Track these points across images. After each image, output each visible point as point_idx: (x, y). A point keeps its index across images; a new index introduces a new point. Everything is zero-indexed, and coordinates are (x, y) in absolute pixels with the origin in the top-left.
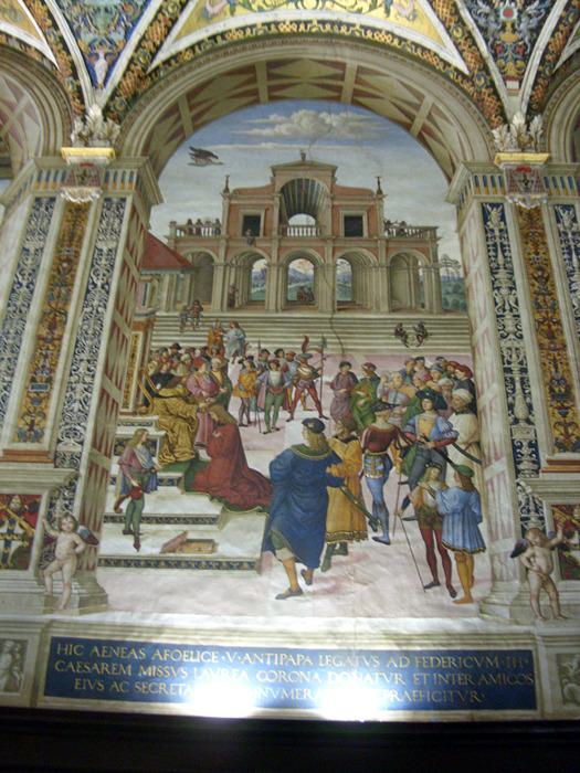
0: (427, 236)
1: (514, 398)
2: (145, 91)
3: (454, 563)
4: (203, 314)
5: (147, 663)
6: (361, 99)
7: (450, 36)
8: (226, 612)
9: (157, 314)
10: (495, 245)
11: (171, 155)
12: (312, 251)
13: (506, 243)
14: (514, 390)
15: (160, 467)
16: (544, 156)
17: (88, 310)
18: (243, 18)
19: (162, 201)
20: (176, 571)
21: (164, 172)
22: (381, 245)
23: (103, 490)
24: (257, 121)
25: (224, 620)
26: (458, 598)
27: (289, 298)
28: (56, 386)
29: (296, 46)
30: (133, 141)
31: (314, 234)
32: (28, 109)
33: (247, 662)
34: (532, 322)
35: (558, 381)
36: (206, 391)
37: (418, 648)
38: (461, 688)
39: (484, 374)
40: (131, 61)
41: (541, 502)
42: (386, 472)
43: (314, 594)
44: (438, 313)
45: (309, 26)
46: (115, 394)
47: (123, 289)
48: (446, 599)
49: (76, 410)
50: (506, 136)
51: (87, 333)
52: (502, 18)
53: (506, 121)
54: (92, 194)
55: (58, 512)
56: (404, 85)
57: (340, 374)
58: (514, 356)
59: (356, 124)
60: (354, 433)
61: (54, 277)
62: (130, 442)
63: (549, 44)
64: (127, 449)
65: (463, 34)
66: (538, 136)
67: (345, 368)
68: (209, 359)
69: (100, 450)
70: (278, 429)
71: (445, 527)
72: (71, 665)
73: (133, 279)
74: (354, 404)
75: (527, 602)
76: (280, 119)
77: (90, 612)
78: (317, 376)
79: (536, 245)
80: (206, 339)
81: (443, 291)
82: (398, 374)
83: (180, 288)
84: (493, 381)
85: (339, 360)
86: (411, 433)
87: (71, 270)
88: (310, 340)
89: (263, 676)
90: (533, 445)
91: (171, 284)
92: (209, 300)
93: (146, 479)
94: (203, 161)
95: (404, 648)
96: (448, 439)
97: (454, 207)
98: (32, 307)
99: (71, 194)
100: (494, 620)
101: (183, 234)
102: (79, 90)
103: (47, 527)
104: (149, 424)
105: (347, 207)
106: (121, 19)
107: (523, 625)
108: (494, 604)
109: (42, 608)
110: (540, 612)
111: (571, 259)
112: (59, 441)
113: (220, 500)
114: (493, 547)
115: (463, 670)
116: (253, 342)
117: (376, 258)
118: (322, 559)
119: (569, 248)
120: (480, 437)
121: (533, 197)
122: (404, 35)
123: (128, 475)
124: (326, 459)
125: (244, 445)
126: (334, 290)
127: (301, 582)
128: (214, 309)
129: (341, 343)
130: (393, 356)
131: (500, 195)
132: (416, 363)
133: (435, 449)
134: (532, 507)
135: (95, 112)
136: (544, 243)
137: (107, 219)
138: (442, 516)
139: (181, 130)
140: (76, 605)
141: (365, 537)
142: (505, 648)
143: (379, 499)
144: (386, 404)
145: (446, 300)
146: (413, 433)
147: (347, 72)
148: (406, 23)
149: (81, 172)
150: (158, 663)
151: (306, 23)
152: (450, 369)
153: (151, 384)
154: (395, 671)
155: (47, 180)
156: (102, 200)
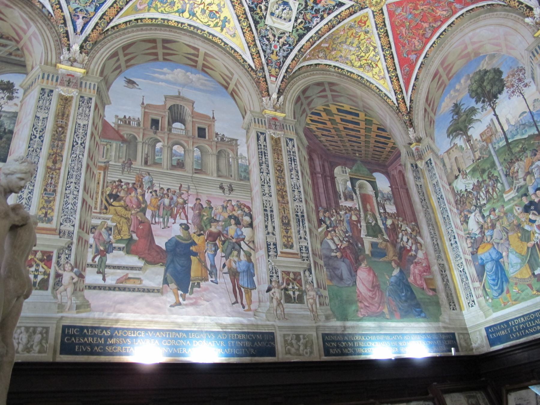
0: (233, 143)
4: (133, 166)
5: (111, 337)
6: (206, 69)
7: (250, 50)
9: (110, 163)
11: (115, 79)
14: (268, 219)
17: (74, 156)
18: (153, 14)
19: (110, 103)
20: (123, 293)
21: (111, 88)
30: (95, 67)
32: (34, 34)
37: (230, 330)
38: (247, 348)
40: (97, 24)
42: (216, 251)
43: (186, 305)
46: (89, 201)
48: (241, 309)
49: (70, 208)
52: (273, 48)
54: (73, 92)
55: (63, 261)
56: (225, 66)
58: (268, 204)
59: (204, 81)
60: (202, 232)
61: (54, 135)
62: (98, 227)
63: (290, 64)
67: (198, 201)
68: (136, 189)
72: (73, 339)
73: (97, 143)
74: (202, 218)
76: (169, 71)
77: (81, 312)
78: (186, 203)
79: (278, 155)
89: (165, 342)
90: (275, 244)
91: (116, 148)
92: (135, 159)
93: (107, 246)
94: (131, 86)
95: (225, 330)
96: (241, 238)
97: (245, 131)
98: (42, 150)
99: (63, 91)
102: (67, 32)
103: (57, 268)
105: (199, 123)
108: (259, 312)
109: (57, 310)
111: (291, 164)
112: (61, 224)
113: (143, 259)
115: (248, 340)
117: (212, 151)
118: (189, 289)
119: (291, 158)
122: (227, 42)
123: (98, 244)
125: (154, 233)
127: (181, 299)
128: (138, 164)
129: (196, 189)
131: (264, 129)
133: (236, 242)
134: (274, 271)
135: (76, 47)
136: (281, 155)
138: (239, 273)
139: (119, 67)
141: (207, 280)
142: (264, 331)
144: (216, 220)
146: (227, 234)
148: (230, 38)
149: (68, 79)
150: (116, 337)
151: (182, 24)
152: (242, 207)
153: (108, 199)
155: (48, 79)
156: (79, 97)
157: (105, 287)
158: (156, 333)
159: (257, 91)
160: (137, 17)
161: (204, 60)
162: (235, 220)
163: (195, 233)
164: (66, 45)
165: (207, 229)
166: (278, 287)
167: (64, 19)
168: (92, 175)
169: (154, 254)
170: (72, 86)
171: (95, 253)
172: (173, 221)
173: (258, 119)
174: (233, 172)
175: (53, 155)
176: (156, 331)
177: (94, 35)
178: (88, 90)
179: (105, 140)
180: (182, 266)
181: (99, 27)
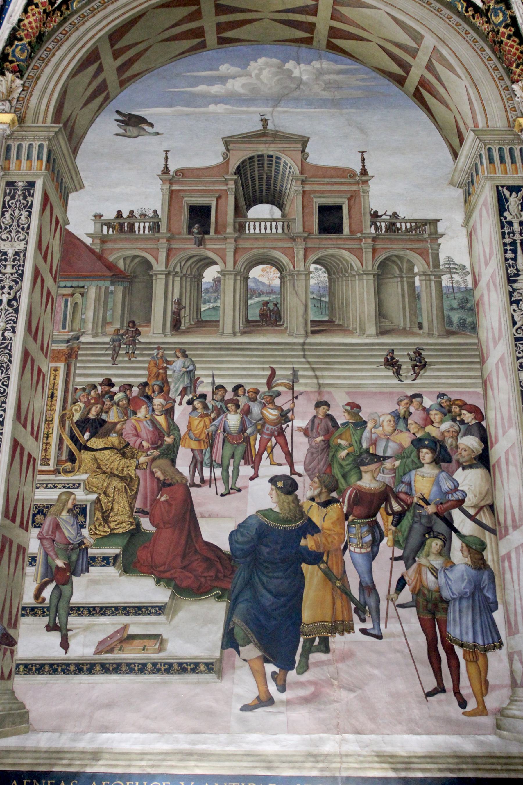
4: (141, 339)
9: (82, 339)
10: (513, 243)
11: (92, 121)
12: (277, 254)
15: (92, 541)
19: (82, 186)
20: (114, 677)
21: (83, 147)
22: (367, 244)
23: (19, 573)
26: (469, 708)
27: (250, 319)
30: (40, 100)
31: (280, 230)
36: (147, 441)
37: (420, 775)
39: (499, 416)
42: (375, 544)
43: (288, 703)
44: (440, 336)
47: (37, 310)
57: (315, 417)
60: (334, 494)
62: (52, 509)
67: (322, 410)
68: (149, 398)
69: (13, 520)
70: (239, 490)
71: (451, 616)
73: (49, 293)
74: (334, 456)
80: (146, 372)
81: (446, 307)
82: (389, 417)
83: (110, 305)
84: (510, 427)
86: (406, 493)
88: (278, 373)
91: (98, 299)
92: (148, 321)
93: (74, 557)
94: (133, 131)
95: (403, 774)
100: (515, 739)
101: (111, 232)
104: (76, 486)
108: (514, 717)
114: (512, 642)
116: (207, 376)
118: (297, 658)
120: (493, 498)
123: (51, 553)
124: (300, 528)
125: (197, 510)
126: (306, 306)
127: (272, 688)
129: (316, 377)
133: (436, 514)
137: (10, 211)
138: (448, 602)
139: (103, 87)
143: (367, 579)
144: (374, 455)
145: (449, 317)
146: (409, 494)
152: (456, 409)
157: (68, 665)
159: (496, 69)
162: (433, 451)
163: (312, 499)
165: (349, 486)
169: (199, 566)
173: (501, 150)
174: (425, 315)
177: (32, 19)
178: (24, 163)
179: (69, 284)
180: (277, 595)
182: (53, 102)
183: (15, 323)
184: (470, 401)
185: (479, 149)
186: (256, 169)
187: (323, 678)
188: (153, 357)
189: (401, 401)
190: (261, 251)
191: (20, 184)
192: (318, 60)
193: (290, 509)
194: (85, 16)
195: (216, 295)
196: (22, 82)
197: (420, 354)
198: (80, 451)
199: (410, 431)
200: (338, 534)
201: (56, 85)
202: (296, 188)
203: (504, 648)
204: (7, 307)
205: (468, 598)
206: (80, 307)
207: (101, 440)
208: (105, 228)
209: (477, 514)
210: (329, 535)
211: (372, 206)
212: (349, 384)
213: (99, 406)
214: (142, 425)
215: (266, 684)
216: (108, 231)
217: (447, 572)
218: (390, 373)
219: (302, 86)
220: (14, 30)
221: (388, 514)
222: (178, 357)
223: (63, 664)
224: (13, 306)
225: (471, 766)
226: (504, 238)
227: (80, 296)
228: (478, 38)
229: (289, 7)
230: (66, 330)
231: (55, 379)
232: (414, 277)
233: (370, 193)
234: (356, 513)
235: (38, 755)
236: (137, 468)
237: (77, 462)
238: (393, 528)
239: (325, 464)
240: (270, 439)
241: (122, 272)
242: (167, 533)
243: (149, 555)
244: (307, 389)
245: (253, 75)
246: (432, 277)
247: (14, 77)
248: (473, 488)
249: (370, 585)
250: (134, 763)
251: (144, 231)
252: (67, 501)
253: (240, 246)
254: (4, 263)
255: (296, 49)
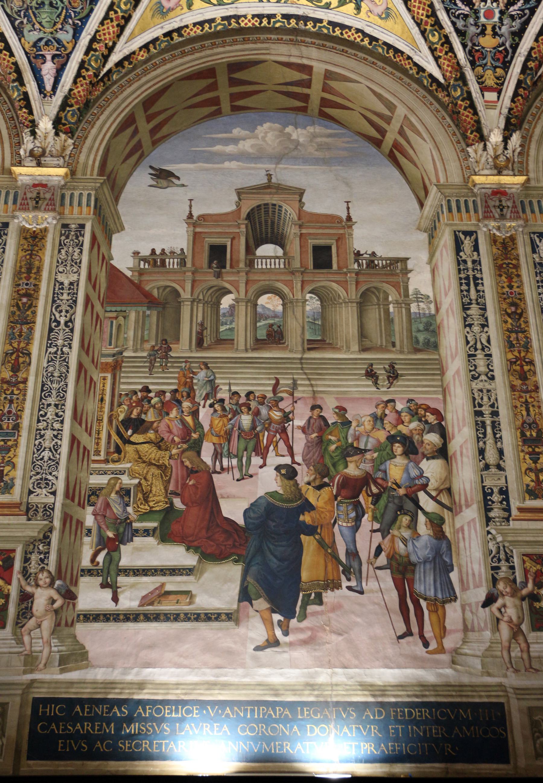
1: (485, 443)
2: (98, 98)
3: (426, 612)
4: (172, 354)
5: (130, 720)
8: (205, 664)
9: (125, 354)
10: (467, 278)
11: (130, 174)
12: (280, 285)
13: (478, 276)
14: (485, 434)
15: (135, 517)
16: (521, 179)
17: (53, 350)
19: (123, 229)
20: (154, 625)
23: (78, 542)
24: (220, 136)
25: (204, 674)
26: (431, 648)
28: (24, 433)
29: (259, 45)
30: (88, 156)
31: (282, 266)
33: (228, 716)
34: (504, 361)
35: (530, 425)
36: (178, 437)
37: (393, 700)
39: (455, 417)
40: (82, 65)
41: (512, 551)
42: (358, 519)
43: (291, 644)
44: (409, 353)
45: (272, 20)
46: (86, 440)
48: (419, 649)
49: (46, 459)
50: (481, 156)
51: (52, 376)
52: (483, 20)
53: (483, 139)
55: (33, 567)
57: (311, 417)
58: (485, 399)
60: (326, 480)
61: (13, 313)
62: (104, 491)
63: (532, 49)
64: (101, 499)
65: (440, 39)
66: (516, 154)
67: (316, 412)
68: (179, 402)
70: (251, 476)
71: (417, 576)
73: (98, 316)
74: (326, 449)
75: (499, 654)
76: (244, 133)
79: (510, 278)
80: (176, 381)
81: (414, 329)
82: (369, 418)
83: (147, 327)
84: (464, 426)
85: (310, 403)
87: (32, 306)
88: (281, 382)
89: (243, 730)
90: (504, 492)
91: (137, 321)
92: (177, 339)
93: (121, 530)
94: (164, 183)
95: (380, 699)
97: (424, 237)
100: (466, 672)
101: (147, 266)
102: (26, 97)
103: (23, 583)
104: (122, 472)
106: (67, 16)
107: (494, 676)
108: (466, 655)
110: (511, 662)
112: (30, 492)
114: (465, 596)
115: (437, 722)
116: (225, 384)
118: (298, 609)
120: (451, 482)
121: (508, 224)
123: (104, 526)
125: (218, 492)
126: (303, 328)
127: (278, 633)
129: (312, 385)
130: (362, 398)
131: (474, 222)
132: (386, 406)
133: (406, 495)
134: (502, 556)
136: (519, 276)
137: (65, 249)
138: (415, 565)
139: (139, 146)
140: (57, 664)
142: (477, 700)
143: (352, 547)
144: (357, 448)
145: (416, 338)
146: (385, 479)
147: (314, 77)
148: (380, 22)
149: (34, 195)
151: (270, 17)
153: (122, 430)
154: (372, 722)
156: (59, 227)
157: (118, 615)
158: (223, 710)
159: (454, 134)
160: (168, 28)
161: (324, 90)
162: (404, 445)
163: (309, 483)
164: (27, 123)
165: (338, 473)
166: (514, 593)
167: (18, 71)
168: (88, 385)
170: (43, 207)
171: (97, 546)
172: (261, 462)
173: (458, 201)
175: (12, 354)
176: (223, 704)
177: (80, 89)
178: (76, 209)
179: (114, 309)
181: (87, 70)
182: (99, 158)
183: (71, 340)
184: (432, 405)
185: (440, 200)
186: (263, 215)
187: (318, 625)
188: (182, 369)
189: (379, 405)
190: (267, 283)
191: (73, 226)
192: (311, 126)
193: (292, 492)
194: (123, 86)
195: (231, 318)
196: (73, 141)
197: (393, 367)
198: (125, 444)
199: (385, 429)
200: (330, 511)
201: (100, 144)
202: (295, 231)
203: (458, 601)
204: (64, 328)
205: (430, 562)
206: (123, 328)
207: (141, 436)
208: (142, 263)
209: (437, 495)
210: (322, 512)
211: (355, 246)
212: (338, 391)
213: (139, 408)
214: (173, 424)
215: (274, 630)
216: (144, 265)
217: (414, 541)
218: (370, 383)
219: (299, 147)
220: (66, 99)
221: (369, 496)
222: (202, 369)
223: (114, 614)
224: (69, 326)
225: (432, 693)
226: (460, 273)
227: (123, 319)
228: (440, 109)
229: (288, 80)
230: (112, 347)
231: (104, 386)
232: (388, 305)
233: (354, 236)
234: (343, 495)
235: (95, 686)
236: (170, 458)
237: (123, 453)
238: (372, 507)
239: (318, 455)
240: (275, 436)
241: (155, 299)
242: (195, 511)
243: (181, 528)
244: (304, 395)
245: (260, 137)
246: (403, 305)
247: (66, 138)
248: (434, 475)
249: (354, 551)
250: (171, 691)
251: (173, 266)
252: (115, 485)
253: (250, 278)
254: (61, 291)
255: (294, 116)
